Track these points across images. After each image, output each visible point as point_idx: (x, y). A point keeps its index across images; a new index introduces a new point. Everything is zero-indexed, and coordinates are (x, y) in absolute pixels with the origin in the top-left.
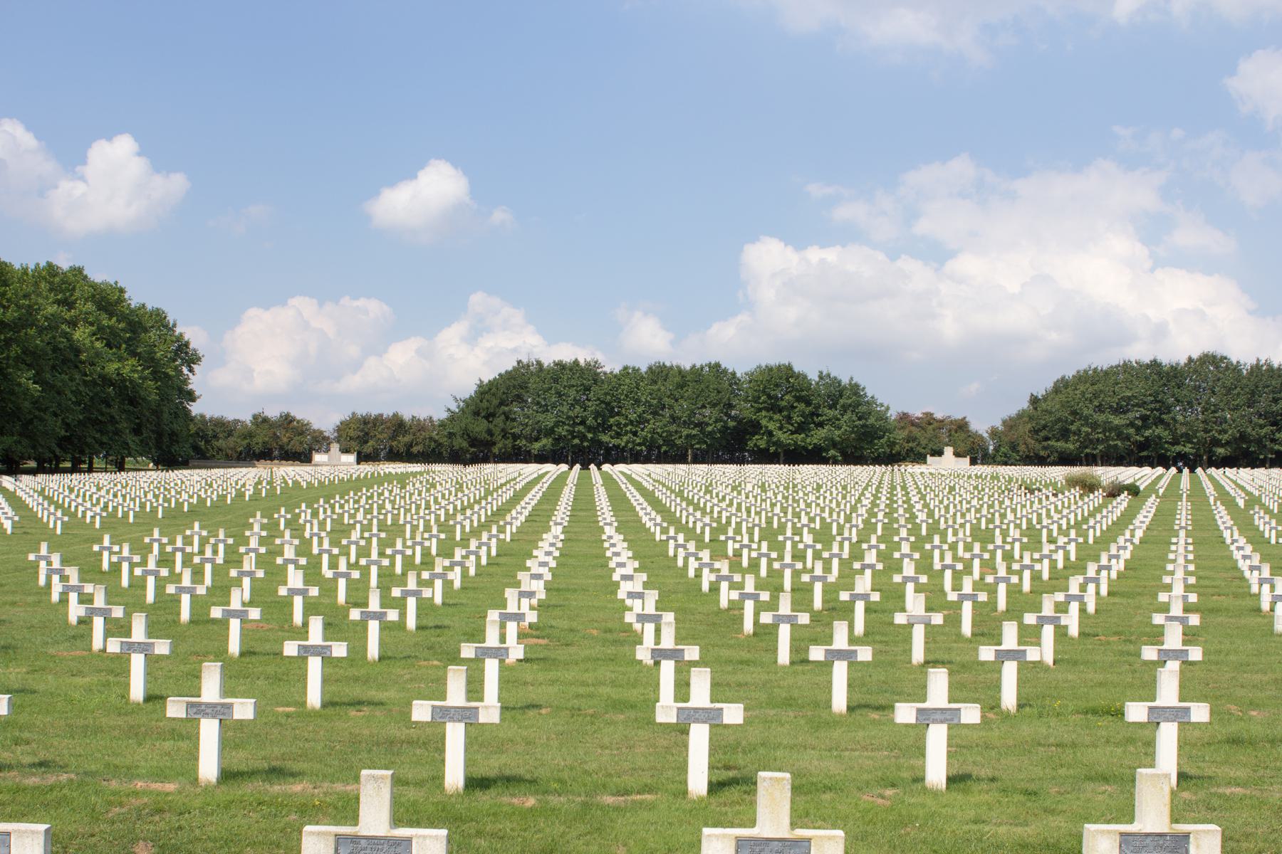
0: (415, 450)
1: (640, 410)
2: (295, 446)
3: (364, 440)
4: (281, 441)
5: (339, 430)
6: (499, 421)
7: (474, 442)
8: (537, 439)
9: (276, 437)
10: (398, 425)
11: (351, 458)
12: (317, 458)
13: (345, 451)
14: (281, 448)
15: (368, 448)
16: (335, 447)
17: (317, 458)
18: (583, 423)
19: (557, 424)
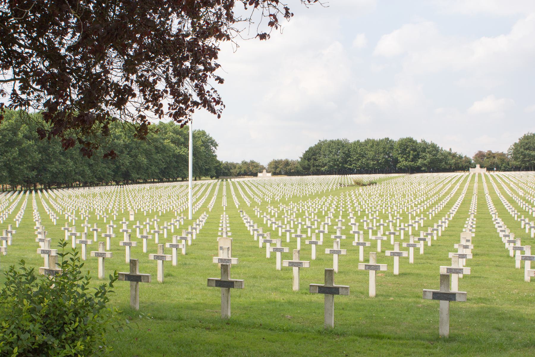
0: (292, 171)
1: (357, 156)
2: (254, 171)
3: (276, 167)
4: (250, 170)
5: (270, 164)
6: (312, 161)
7: (304, 168)
8: (323, 167)
9: (248, 168)
10: (287, 163)
11: (270, 174)
12: (259, 174)
13: (267, 172)
14: (250, 171)
15: (278, 170)
16: (264, 171)
17: (259, 174)
18: (338, 161)
19: (329, 162)
